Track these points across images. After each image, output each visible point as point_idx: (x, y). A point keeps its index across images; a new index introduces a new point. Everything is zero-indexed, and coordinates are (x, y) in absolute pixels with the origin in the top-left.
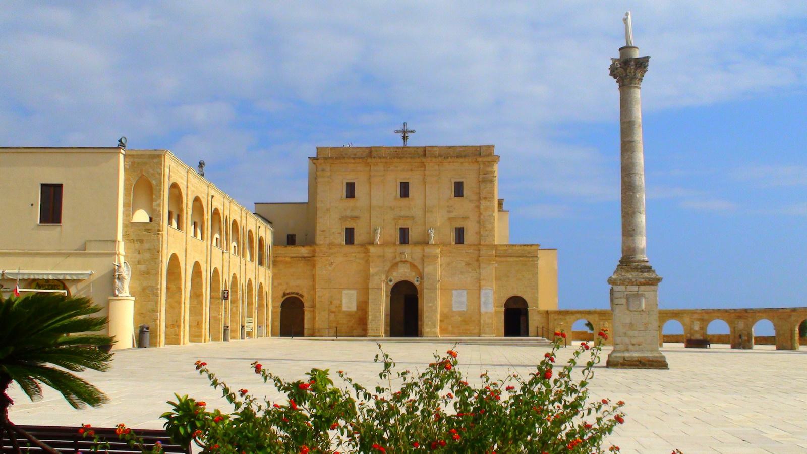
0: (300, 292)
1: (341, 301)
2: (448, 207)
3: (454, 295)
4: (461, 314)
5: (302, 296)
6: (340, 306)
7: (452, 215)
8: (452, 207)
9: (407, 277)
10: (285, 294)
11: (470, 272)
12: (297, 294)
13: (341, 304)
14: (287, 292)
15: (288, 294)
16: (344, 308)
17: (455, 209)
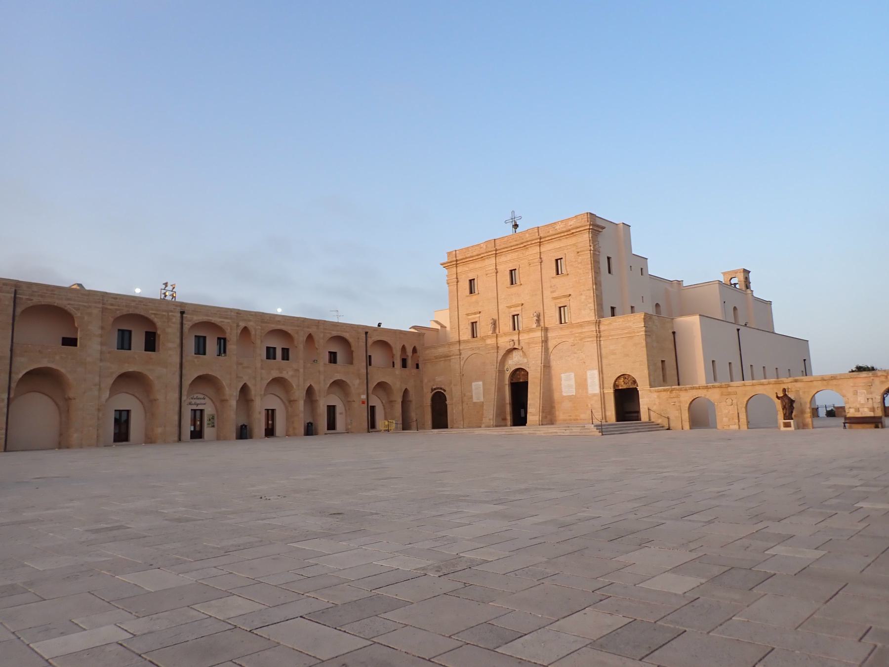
0: (443, 387)
1: (472, 393)
2: (551, 287)
3: (563, 379)
4: (571, 398)
5: (445, 391)
6: (471, 397)
7: (555, 295)
8: (554, 286)
9: (520, 364)
10: (432, 390)
11: (575, 353)
12: (441, 389)
13: (472, 396)
14: (434, 387)
15: (435, 389)
16: (475, 400)
17: (557, 287)
